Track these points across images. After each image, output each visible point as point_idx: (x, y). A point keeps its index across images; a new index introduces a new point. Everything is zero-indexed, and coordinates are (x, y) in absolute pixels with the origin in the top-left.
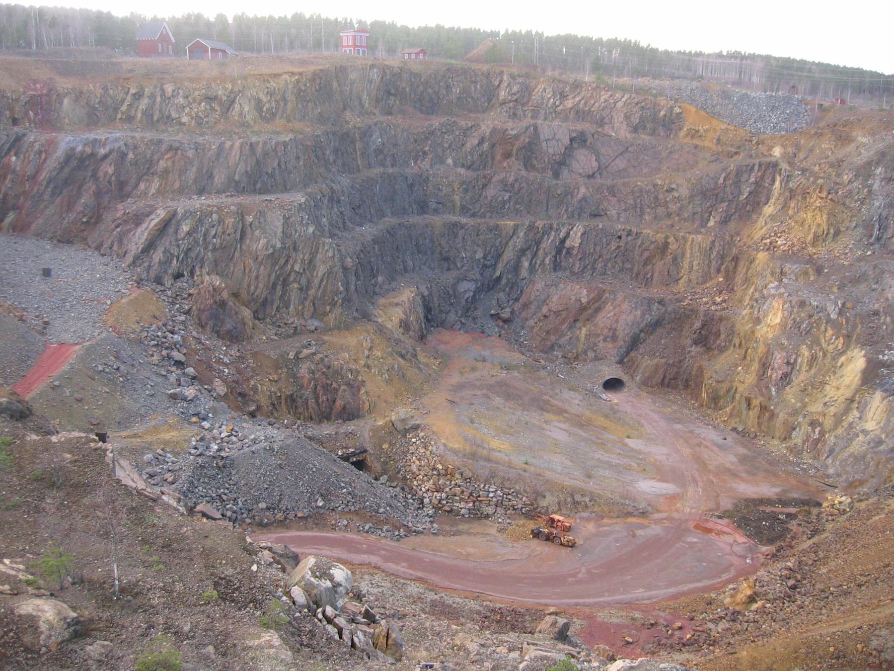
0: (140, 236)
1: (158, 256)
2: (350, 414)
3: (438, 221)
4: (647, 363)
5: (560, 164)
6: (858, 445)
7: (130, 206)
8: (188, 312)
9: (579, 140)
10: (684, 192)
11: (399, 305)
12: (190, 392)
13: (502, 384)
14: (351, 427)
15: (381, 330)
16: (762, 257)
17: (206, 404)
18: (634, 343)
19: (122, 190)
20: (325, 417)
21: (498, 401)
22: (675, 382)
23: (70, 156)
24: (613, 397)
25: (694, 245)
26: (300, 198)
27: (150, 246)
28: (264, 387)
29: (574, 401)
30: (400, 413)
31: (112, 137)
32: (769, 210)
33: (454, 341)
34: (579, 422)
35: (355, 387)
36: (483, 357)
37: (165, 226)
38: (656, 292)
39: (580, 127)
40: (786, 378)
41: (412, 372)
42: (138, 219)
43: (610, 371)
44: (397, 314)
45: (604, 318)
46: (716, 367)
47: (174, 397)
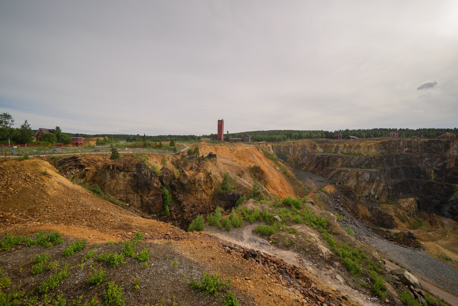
7: (329, 168)
8: (342, 191)
12: (341, 209)
42: (331, 171)
47: (337, 209)
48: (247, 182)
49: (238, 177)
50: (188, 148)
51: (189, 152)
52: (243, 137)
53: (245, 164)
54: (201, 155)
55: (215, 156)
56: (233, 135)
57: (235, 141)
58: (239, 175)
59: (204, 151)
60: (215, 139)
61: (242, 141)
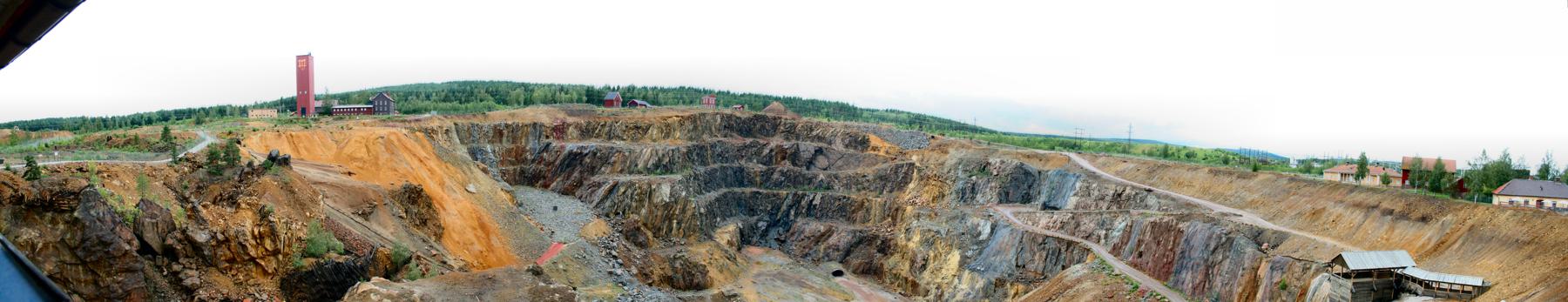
0: (601, 192)
1: (608, 203)
2: (699, 287)
3: (748, 190)
4: (855, 261)
5: (810, 163)
6: (959, 297)
7: (596, 178)
9: (819, 151)
10: (871, 177)
11: (727, 232)
12: (619, 271)
13: (780, 274)
14: (701, 294)
15: (718, 245)
16: (909, 208)
17: (626, 277)
18: (848, 253)
19: (593, 170)
20: (687, 288)
21: (779, 283)
22: (871, 271)
23: (571, 153)
24: (838, 279)
25: (876, 201)
26: (679, 177)
27: (606, 197)
28: (657, 272)
29: (817, 281)
30: (727, 288)
31: (592, 144)
32: (911, 186)
33: (754, 251)
34: (821, 292)
35: (705, 273)
36: (768, 259)
37: (611, 191)
38: (858, 227)
39: (820, 144)
40: (924, 267)
41: (733, 267)
42: (599, 185)
43: (836, 266)
44: (727, 237)
45: (833, 240)
46: (890, 262)
48: (388, 233)
49: (359, 219)
50: (210, 140)
51: (212, 155)
52: (376, 104)
53: (387, 180)
54: (244, 162)
55: (285, 161)
56: (345, 98)
57: (350, 112)
58: (365, 215)
59: (254, 150)
60: (297, 107)
61: (369, 112)
